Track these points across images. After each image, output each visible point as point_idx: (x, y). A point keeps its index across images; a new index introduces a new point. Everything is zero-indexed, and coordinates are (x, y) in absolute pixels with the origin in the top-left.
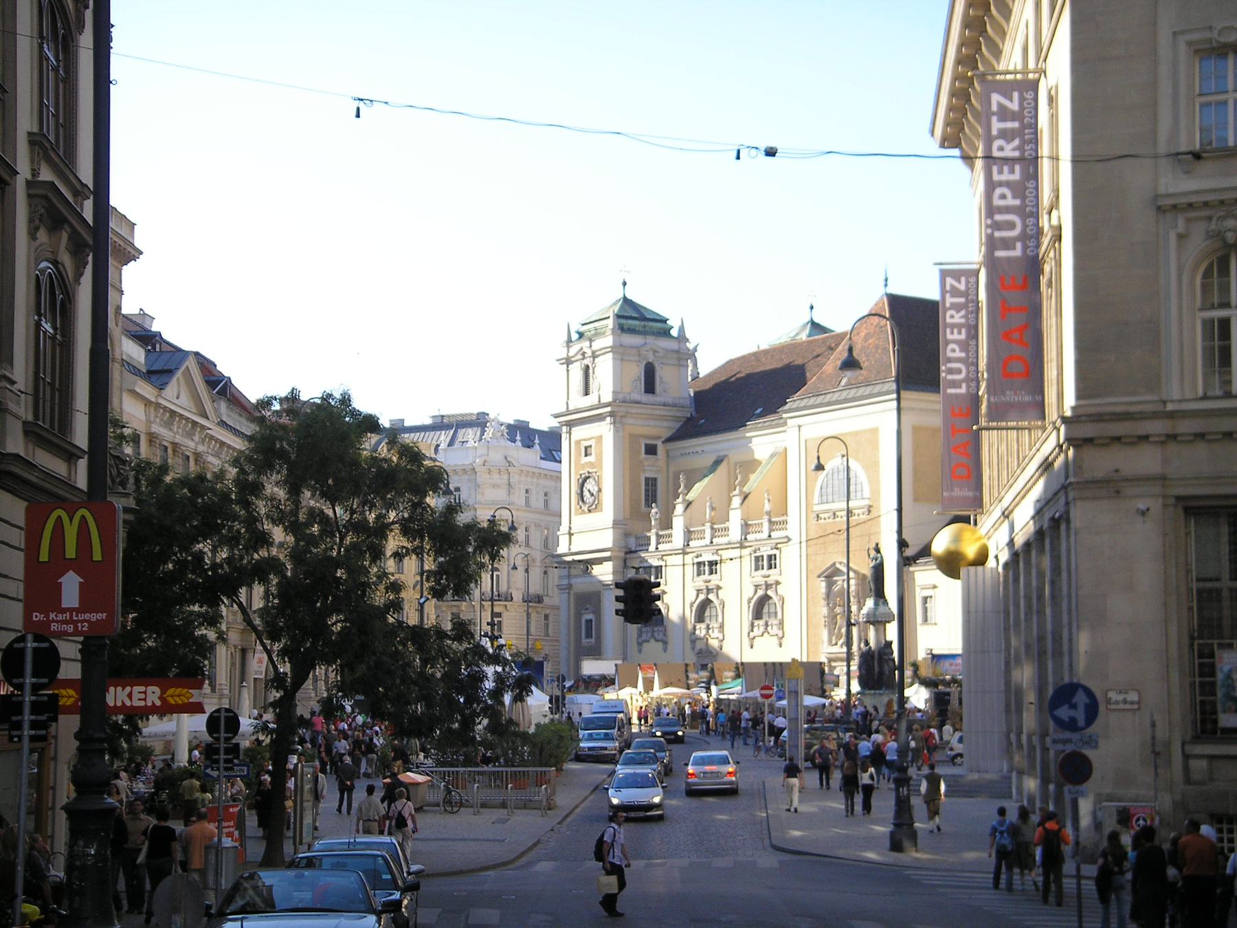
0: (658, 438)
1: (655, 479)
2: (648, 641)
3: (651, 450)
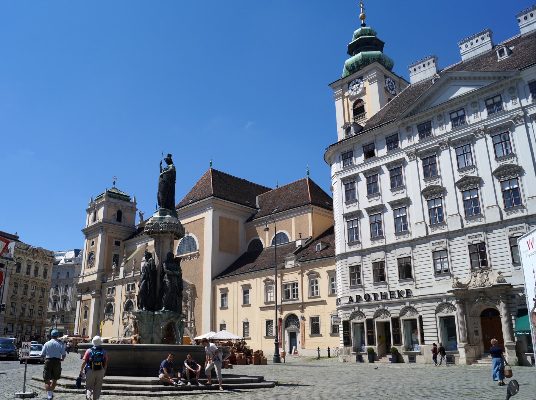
0: (121, 239)
1: (118, 255)
2: (107, 320)
3: (117, 243)
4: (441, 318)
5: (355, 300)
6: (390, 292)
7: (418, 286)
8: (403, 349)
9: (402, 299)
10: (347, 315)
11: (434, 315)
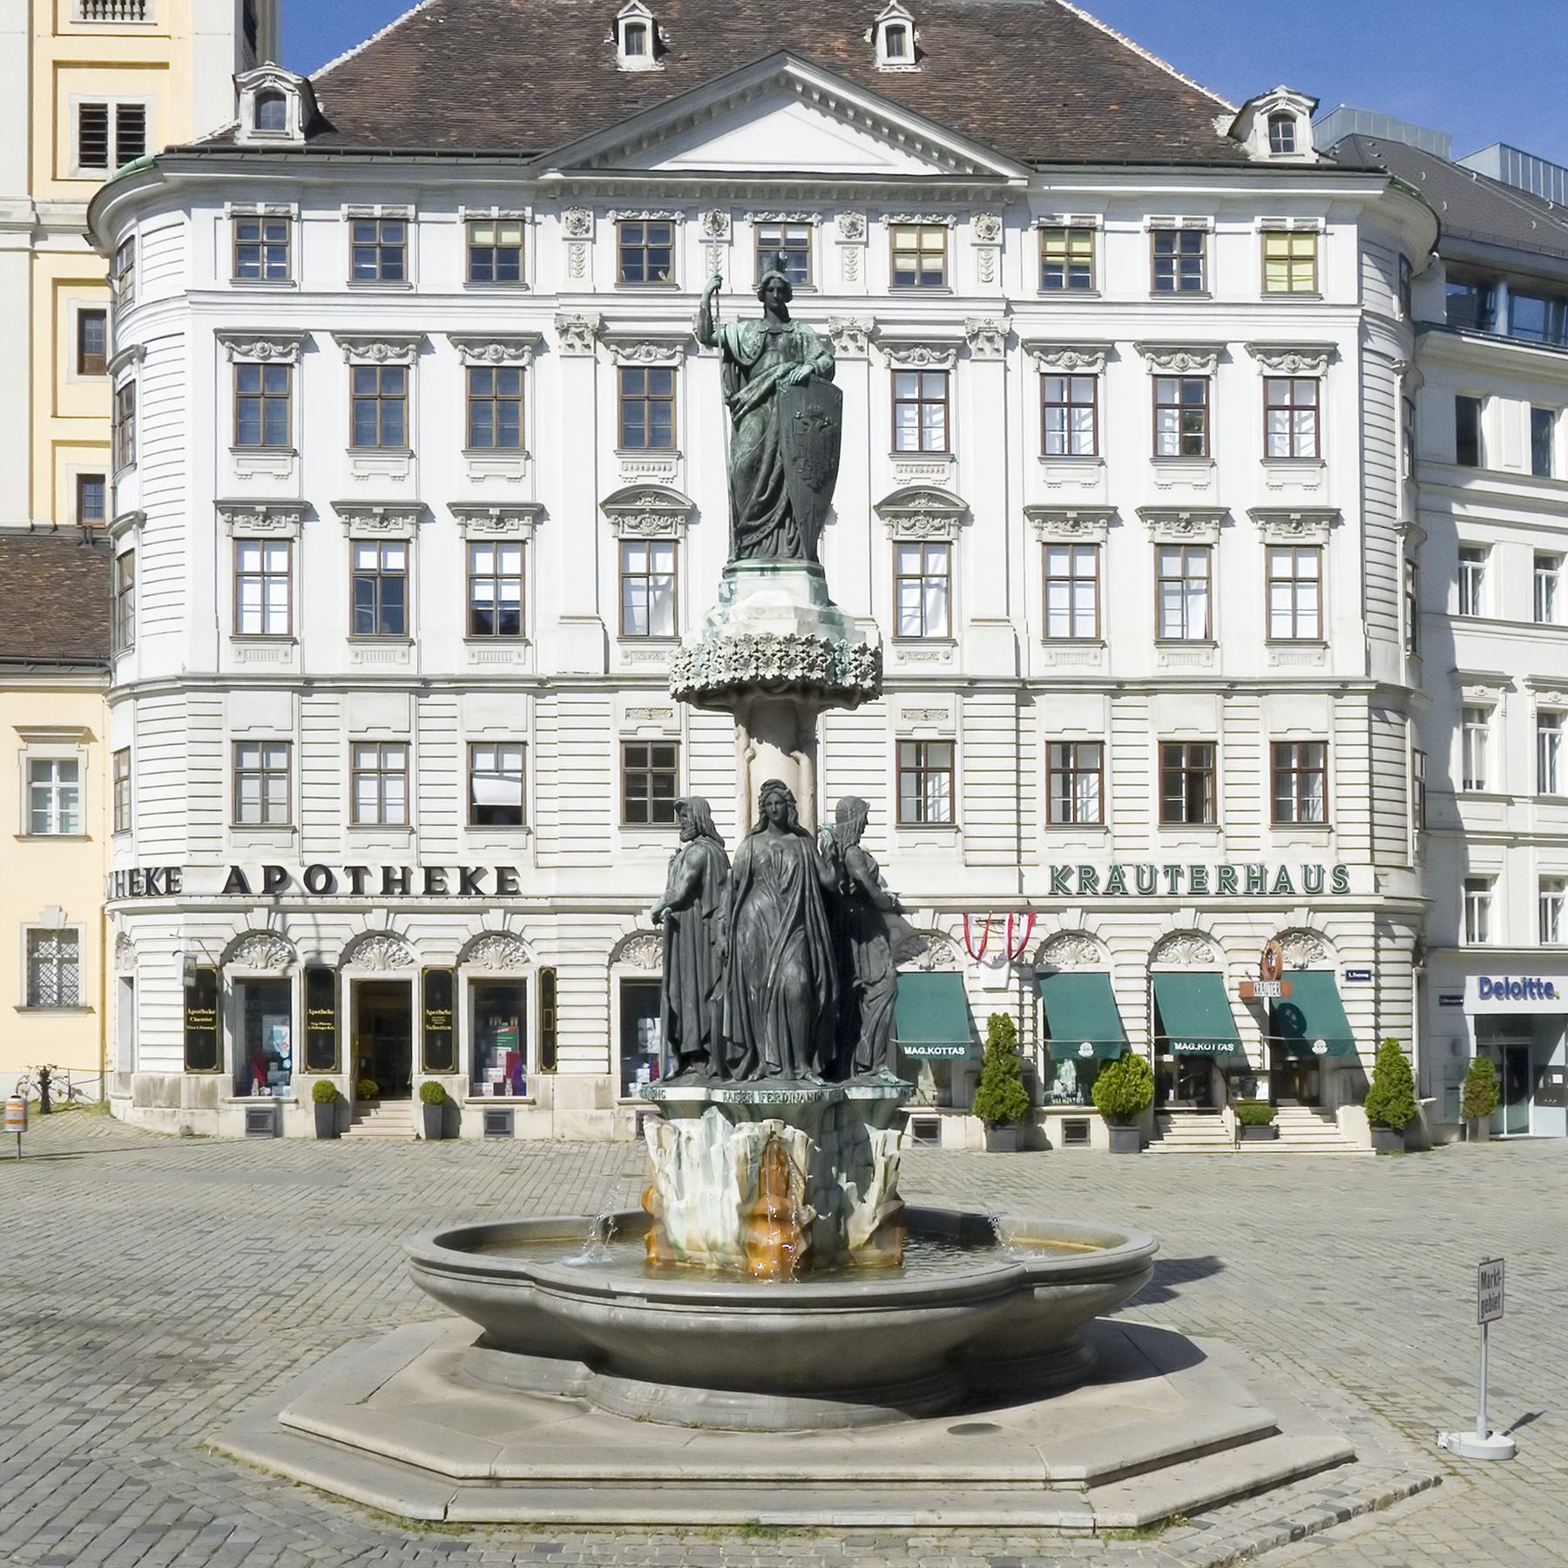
4: (624, 981)
5: (256, 882)
6: (429, 872)
7: (544, 860)
8: (462, 1088)
9: (476, 902)
10: (209, 945)
11: (603, 972)
